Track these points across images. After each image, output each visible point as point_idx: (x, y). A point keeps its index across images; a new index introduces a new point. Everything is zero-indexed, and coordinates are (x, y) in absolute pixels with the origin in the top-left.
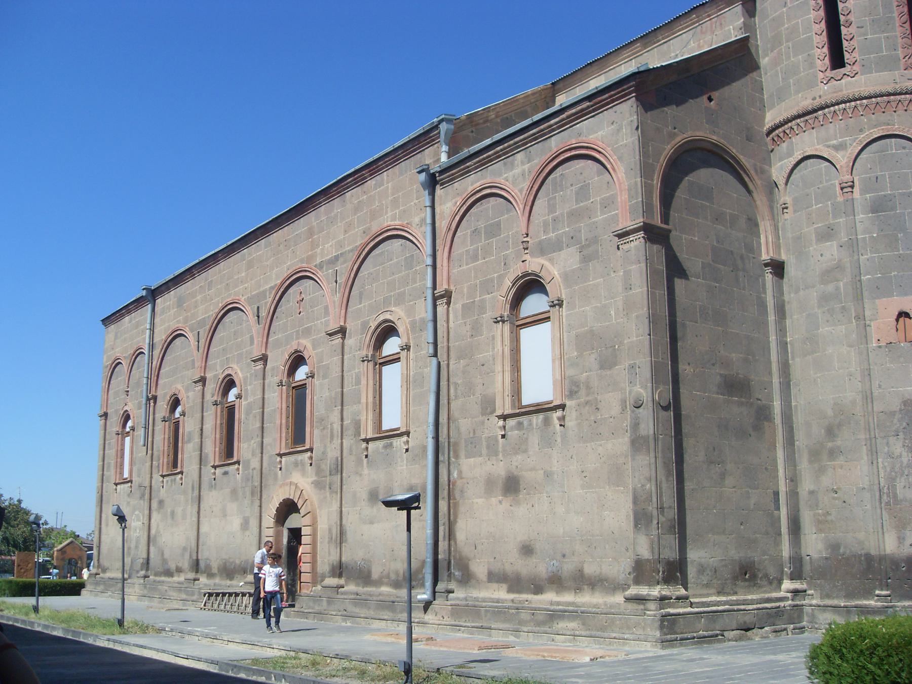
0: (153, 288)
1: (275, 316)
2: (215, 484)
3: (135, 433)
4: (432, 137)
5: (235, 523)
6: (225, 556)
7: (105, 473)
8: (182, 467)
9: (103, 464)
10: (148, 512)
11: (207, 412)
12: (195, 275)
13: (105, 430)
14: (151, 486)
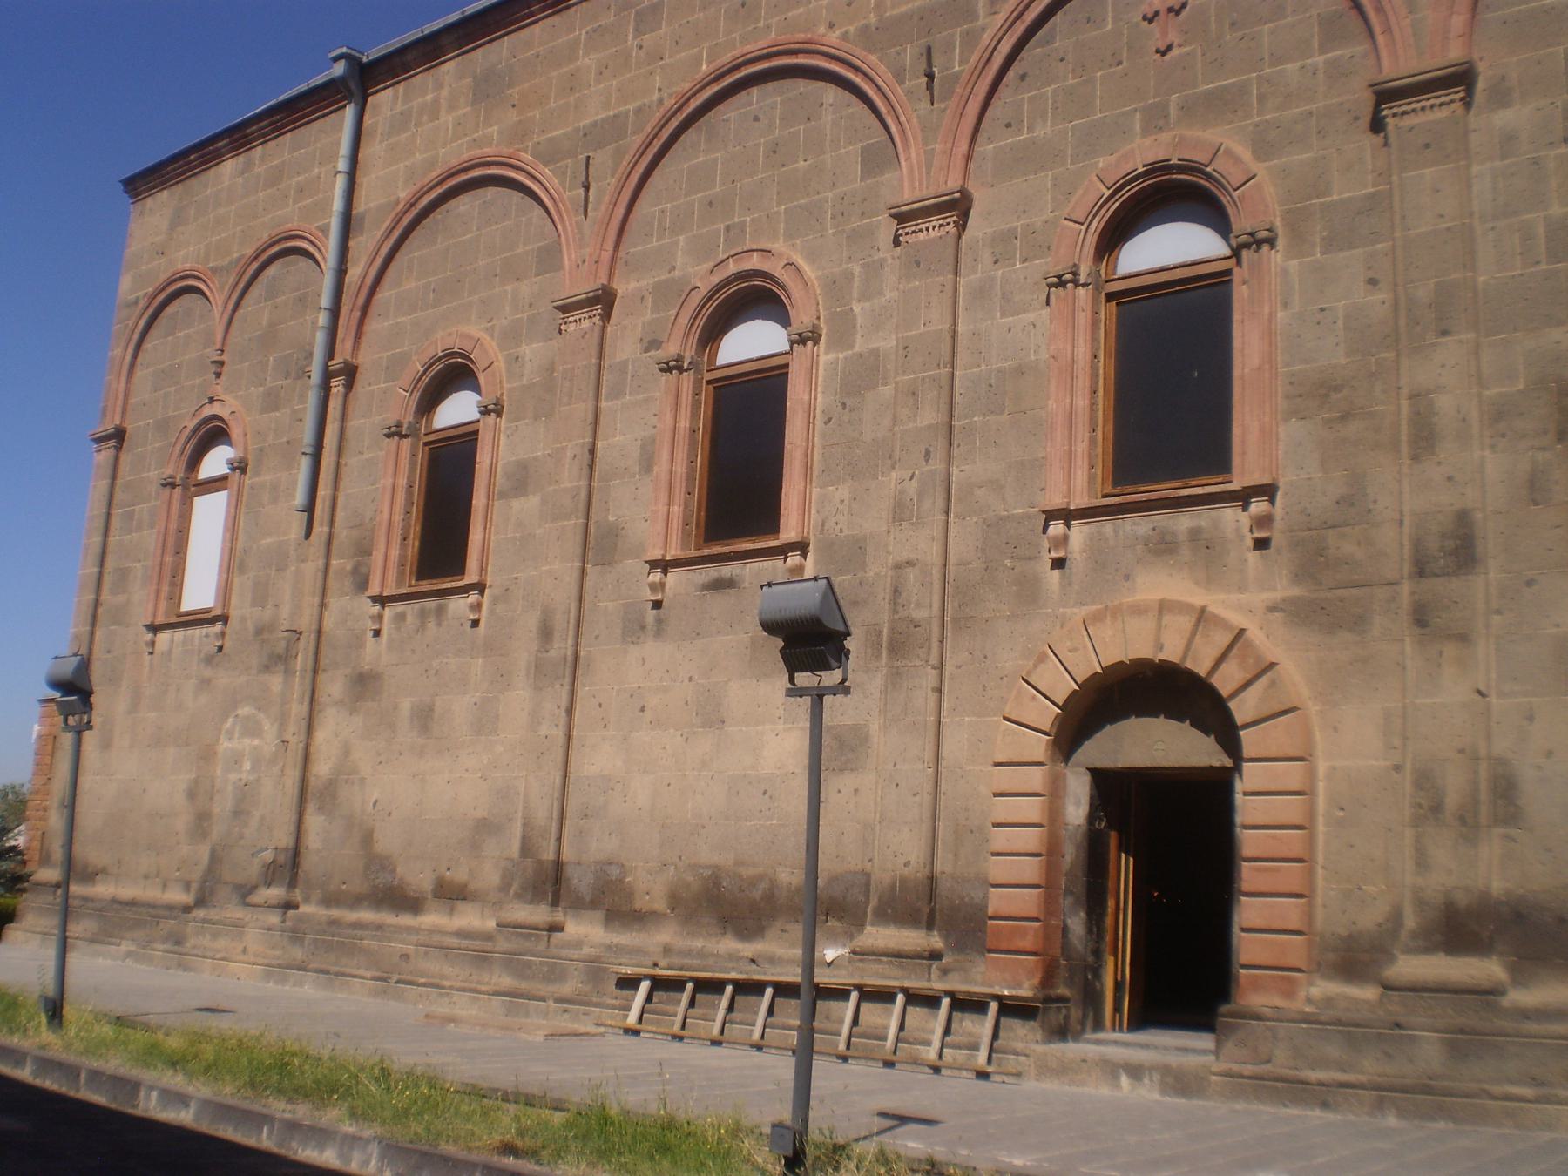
0: (365, 60)
1: (1011, 74)
2: (659, 621)
3: (248, 480)
6: (707, 854)
7: (105, 596)
8: (482, 569)
9: (101, 574)
10: (305, 707)
11: (617, 393)
13: (114, 477)
14: (319, 632)
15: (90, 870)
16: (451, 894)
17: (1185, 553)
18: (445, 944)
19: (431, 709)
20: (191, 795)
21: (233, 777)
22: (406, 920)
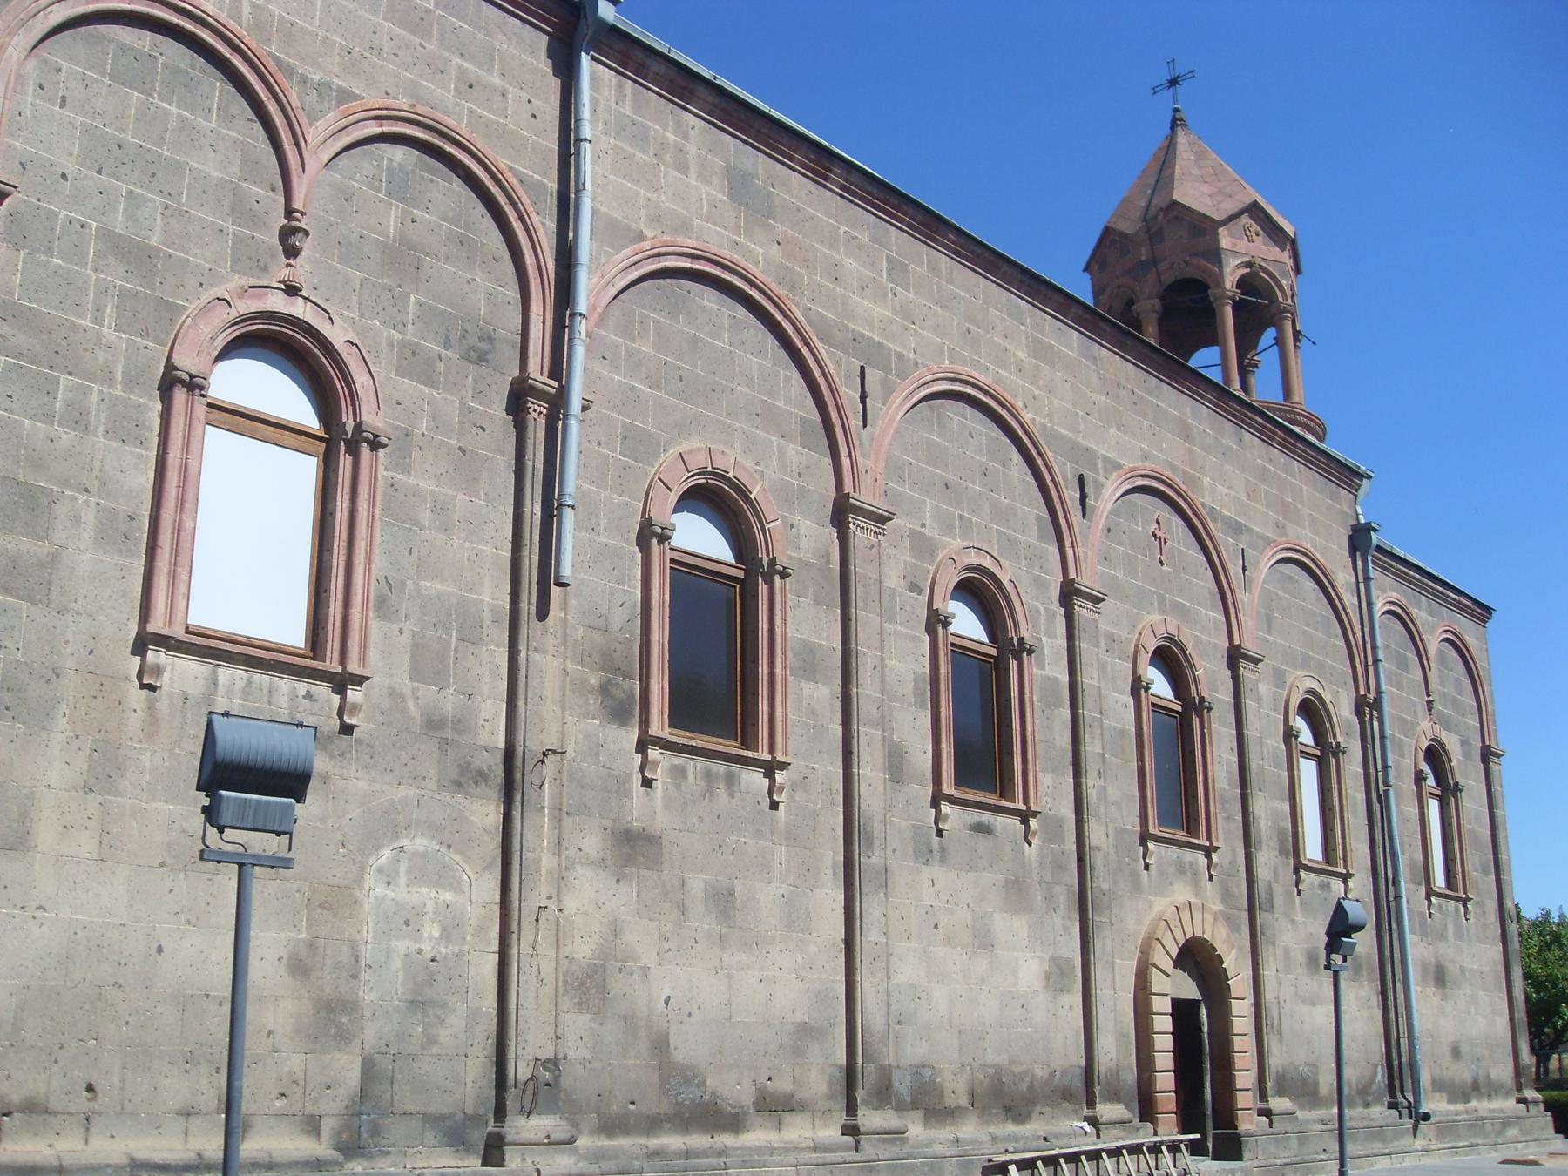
2: (943, 849)
4: (1352, 481)
5: (1029, 971)
6: (994, 1057)
12: (826, 178)
16: (775, 1106)
17: (1189, 874)
18: (828, 1160)
19: (731, 893)
21: (402, 946)
22: (727, 1140)
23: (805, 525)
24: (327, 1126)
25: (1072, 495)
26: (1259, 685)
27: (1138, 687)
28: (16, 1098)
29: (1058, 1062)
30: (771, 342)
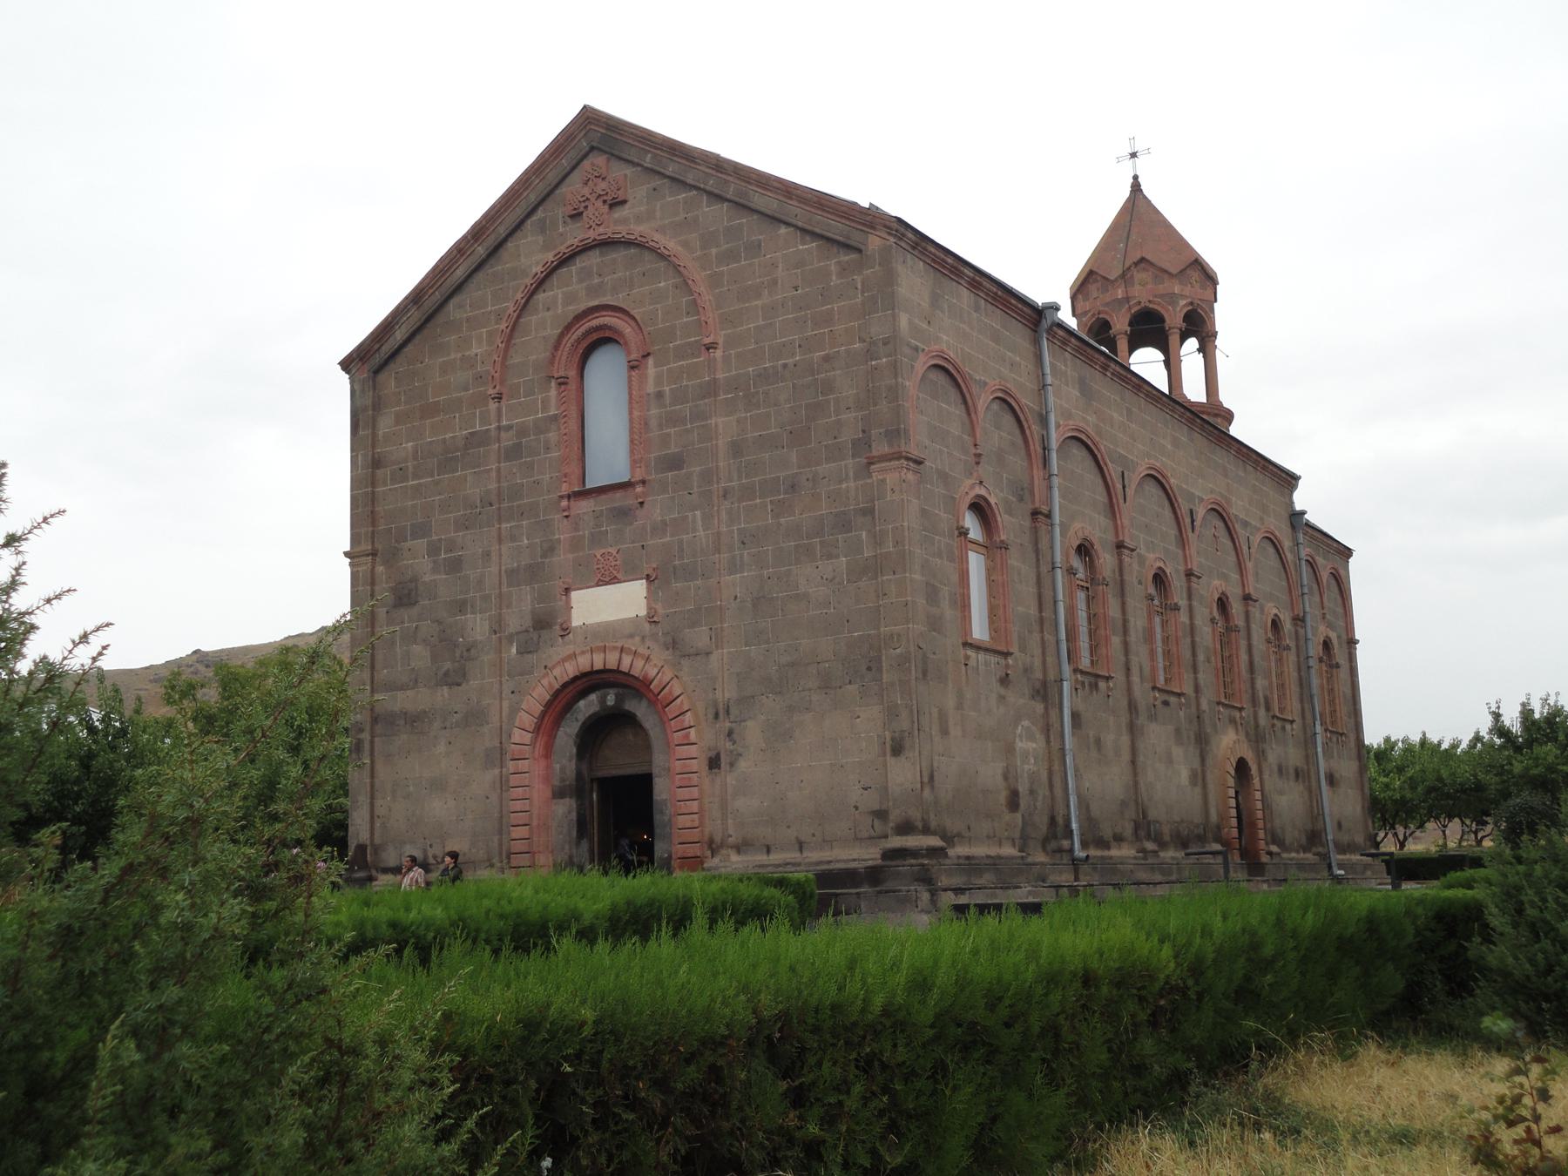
5: (1184, 775)
15: (949, 834)
16: (1119, 839)
19: (1100, 739)
20: (1006, 778)
21: (1026, 767)
22: (1106, 853)
23: (1108, 556)
24: (1017, 842)
25: (1188, 520)
26: (1255, 611)
27: (1213, 620)
28: (955, 831)
29: (1196, 821)
30: (1093, 464)
